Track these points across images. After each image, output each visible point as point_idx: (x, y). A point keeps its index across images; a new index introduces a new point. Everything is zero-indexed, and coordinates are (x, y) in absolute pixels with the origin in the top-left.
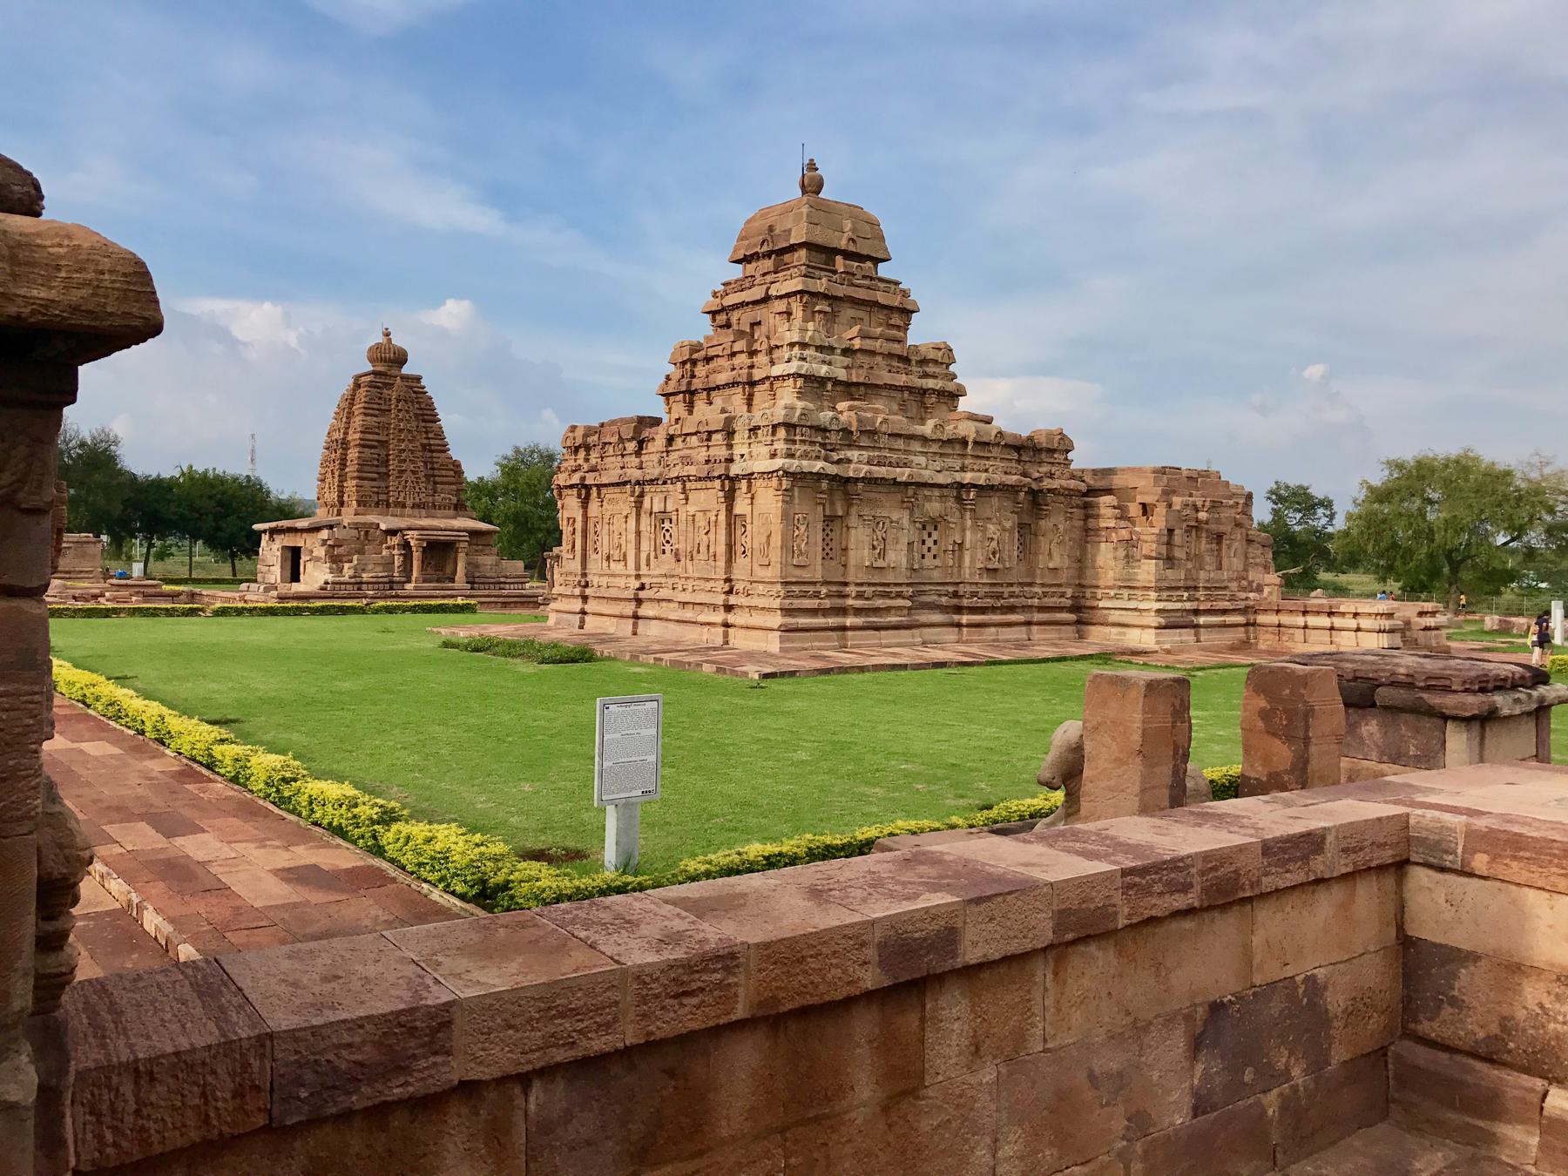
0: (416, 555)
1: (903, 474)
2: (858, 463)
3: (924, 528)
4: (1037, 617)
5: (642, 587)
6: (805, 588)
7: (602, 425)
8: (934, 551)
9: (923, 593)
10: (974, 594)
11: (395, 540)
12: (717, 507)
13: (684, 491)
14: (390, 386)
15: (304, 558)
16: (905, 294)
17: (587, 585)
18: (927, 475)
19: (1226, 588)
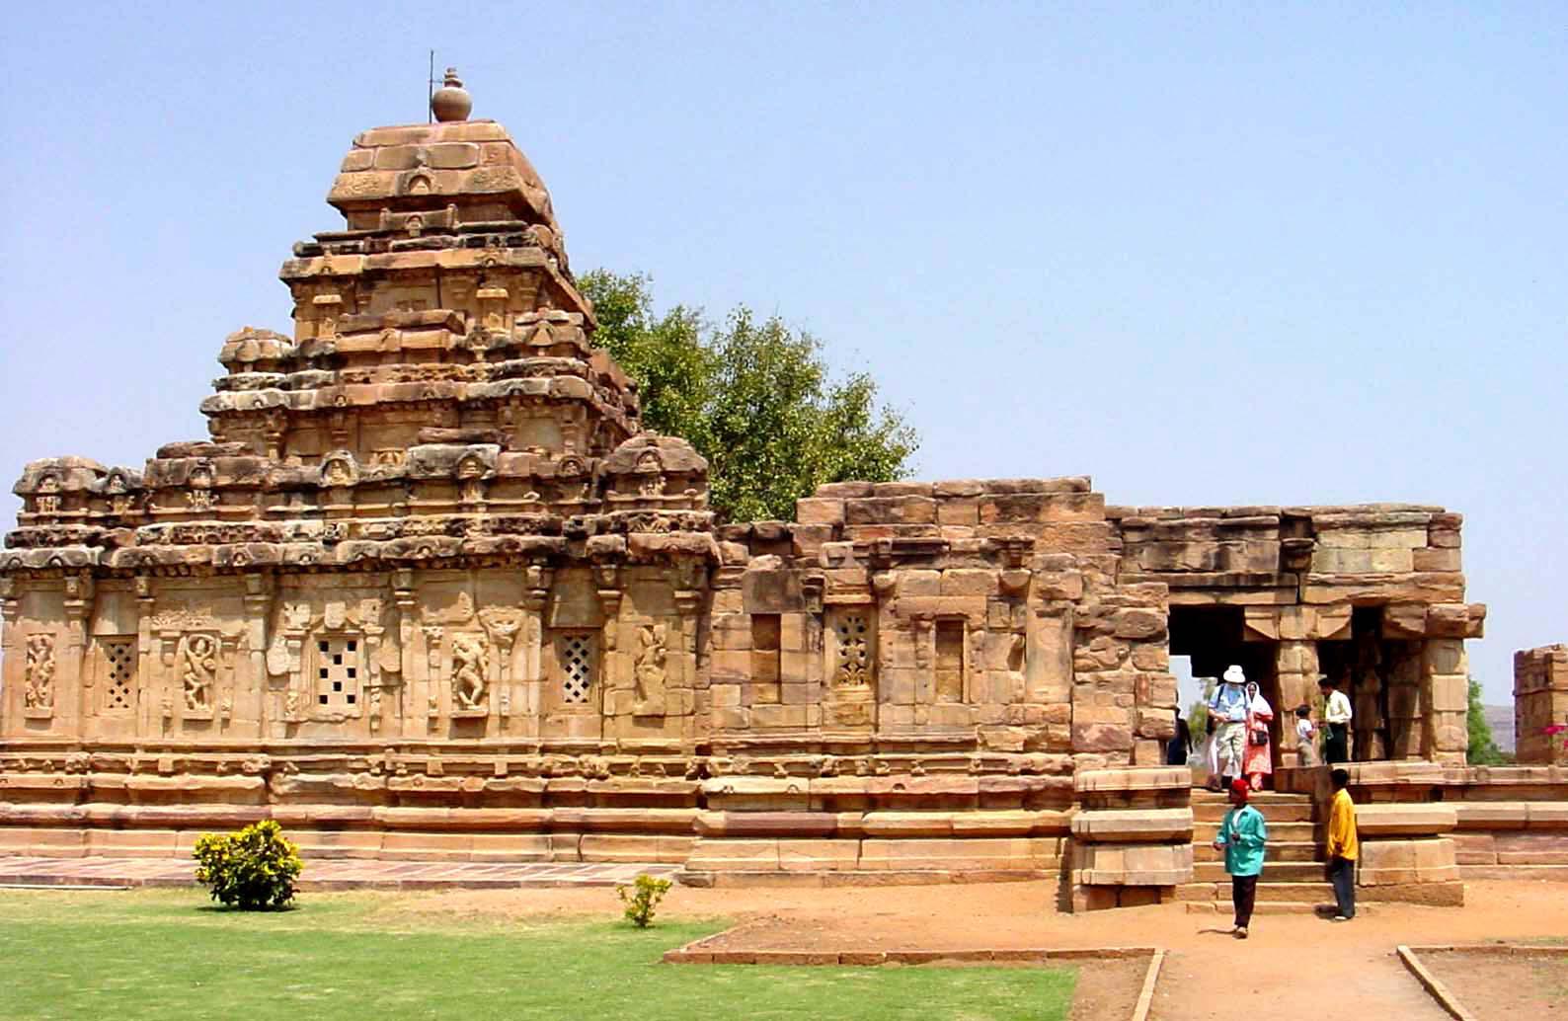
8: (346, 690)
19: (970, 745)
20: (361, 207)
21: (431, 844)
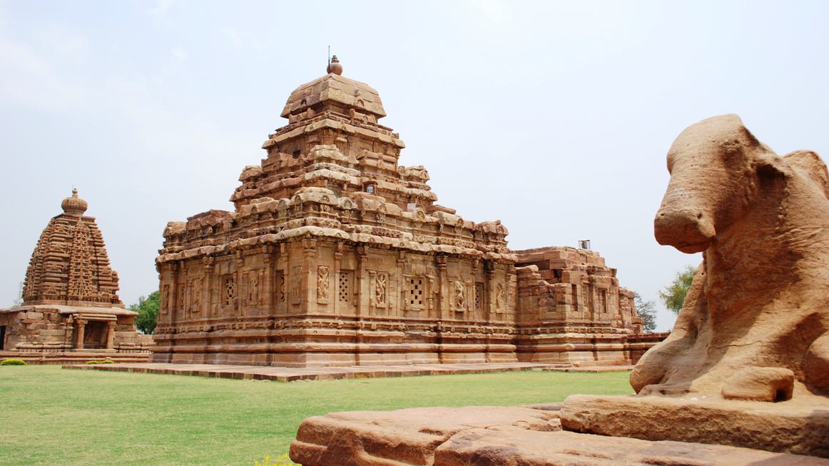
0: (82, 330)
1: (396, 242)
2: (364, 234)
3: (412, 282)
4: (492, 346)
5: (212, 330)
6: (327, 321)
7: (190, 219)
9: (412, 328)
10: (448, 329)
11: (70, 320)
12: (263, 265)
13: (242, 258)
14: (74, 223)
15: (7, 333)
16: (396, 136)
17: (175, 332)
18: (413, 245)
19: (609, 325)
20: (335, 104)
21: (332, 359)
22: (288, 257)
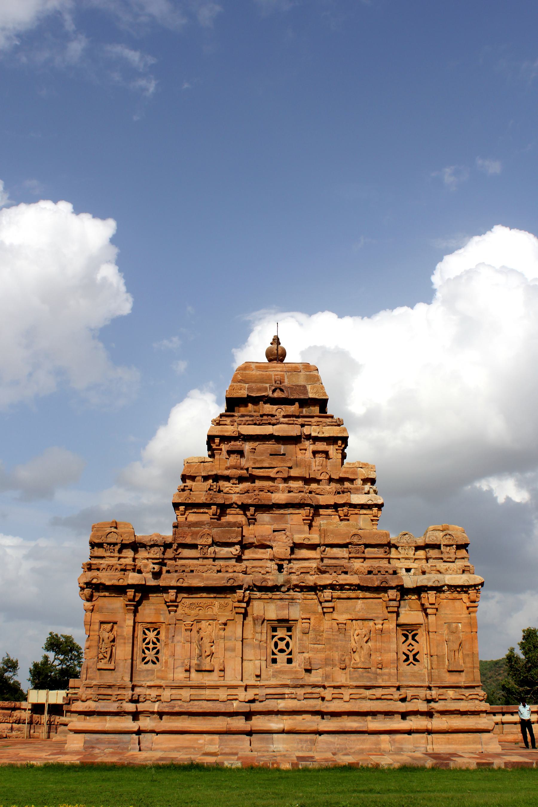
22: (437, 609)
